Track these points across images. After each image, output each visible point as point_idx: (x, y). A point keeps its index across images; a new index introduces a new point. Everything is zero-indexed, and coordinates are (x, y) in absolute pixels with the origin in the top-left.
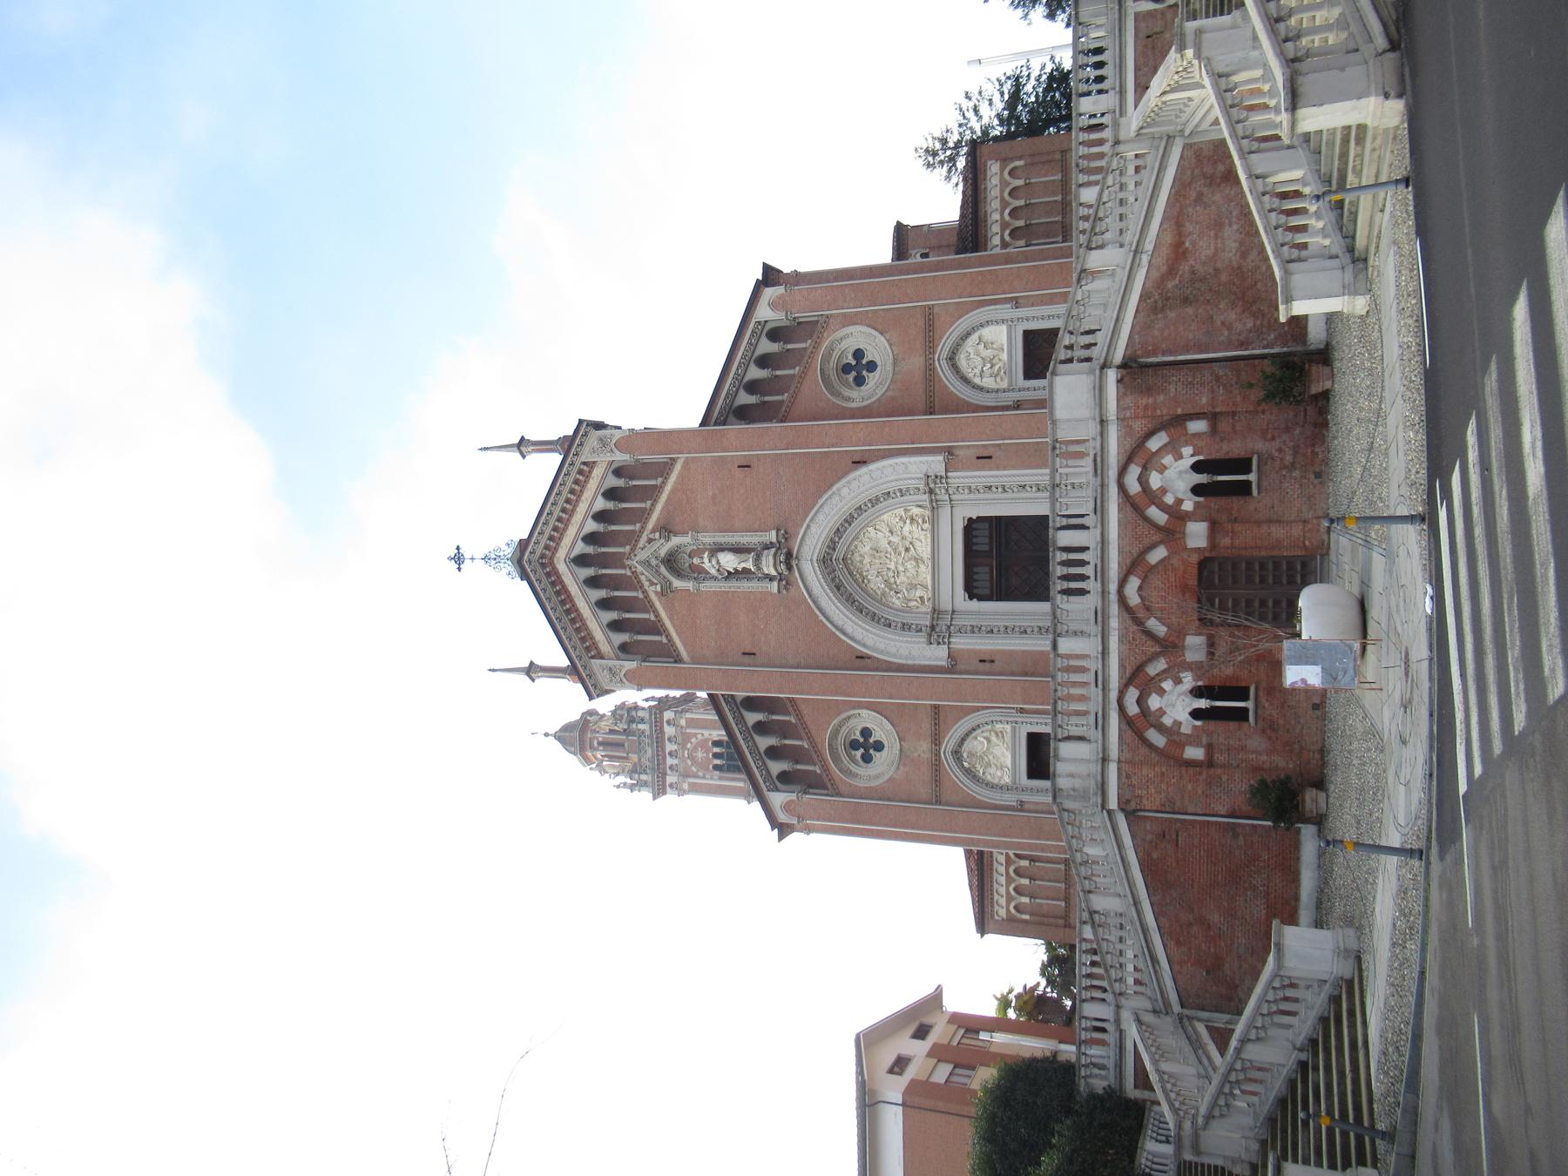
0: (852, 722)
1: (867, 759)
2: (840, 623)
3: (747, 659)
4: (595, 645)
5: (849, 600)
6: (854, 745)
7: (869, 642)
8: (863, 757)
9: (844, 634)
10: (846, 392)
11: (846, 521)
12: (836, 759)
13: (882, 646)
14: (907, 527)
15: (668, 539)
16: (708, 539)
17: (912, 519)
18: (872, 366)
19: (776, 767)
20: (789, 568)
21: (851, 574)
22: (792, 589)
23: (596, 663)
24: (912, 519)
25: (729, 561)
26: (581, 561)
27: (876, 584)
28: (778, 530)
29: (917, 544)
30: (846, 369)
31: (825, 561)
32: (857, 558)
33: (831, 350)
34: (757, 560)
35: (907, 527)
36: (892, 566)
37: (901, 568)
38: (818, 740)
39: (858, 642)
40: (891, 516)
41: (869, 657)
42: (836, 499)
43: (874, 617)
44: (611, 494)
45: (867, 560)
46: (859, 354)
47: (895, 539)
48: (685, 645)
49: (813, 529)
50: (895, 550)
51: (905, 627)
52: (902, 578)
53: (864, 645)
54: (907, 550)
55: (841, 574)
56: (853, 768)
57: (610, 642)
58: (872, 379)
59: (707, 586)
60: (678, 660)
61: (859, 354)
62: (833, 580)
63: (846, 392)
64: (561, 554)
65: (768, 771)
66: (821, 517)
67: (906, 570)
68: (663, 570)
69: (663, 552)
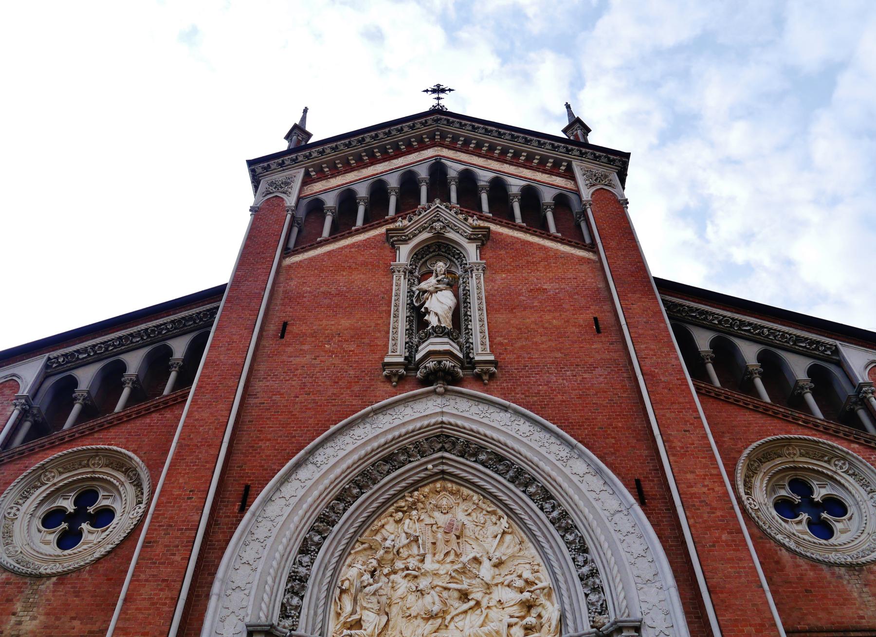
0: (129, 491)
1: (50, 520)
2: (319, 457)
3: (273, 328)
4: (322, 176)
5: (363, 479)
6: (87, 497)
7: (272, 510)
8: (61, 511)
9: (298, 466)
10: (760, 484)
11: (520, 472)
12: (65, 464)
13: (260, 533)
14: (511, 596)
15: (470, 239)
16: (476, 285)
17: (528, 606)
18: (823, 530)
19: (86, 377)
20: (426, 381)
21: (415, 486)
22: (388, 387)
23: (300, 174)
24: (528, 606)
25: (440, 305)
26: (438, 169)
27: (392, 532)
28: (494, 363)
29: (475, 618)
30: (801, 487)
31: (442, 438)
32: (445, 501)
33: (832, 456)
34: (440, 331)
35: (511, 596)
36: (429, 565)
37: (423, 583)
38: (112, 433)
39: (277, 488)
40: (527, 562)
41: (243, 509)
42: (564, 452)
43: (324, 521)
44: (530, 195)
45: (441, 519)
46: (837, 507)
47: (486, 571)
48: (311, 259)
49: (505, 417)
50: (463, 571)
51: (297, 583)
52: (403, 585)
53: (269, 500)
54: (464, 596)
55: (412, 468)
56: (38, 494)
57: (326, 191)
58: (797, 530)
59: (400, 286)
60: (287, 252)
61: (837, 507)
62: (404, 450)
63: (760, 484)
64: (445, 152)
65: (85, 364)
66: (525, 427)
67: (421, 593)
68: (425, 235)
69: (452, 235)
